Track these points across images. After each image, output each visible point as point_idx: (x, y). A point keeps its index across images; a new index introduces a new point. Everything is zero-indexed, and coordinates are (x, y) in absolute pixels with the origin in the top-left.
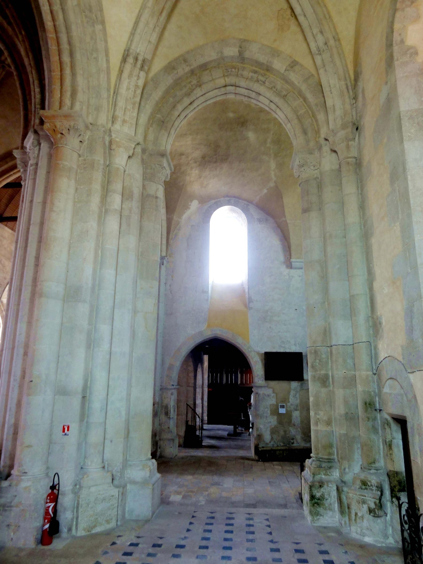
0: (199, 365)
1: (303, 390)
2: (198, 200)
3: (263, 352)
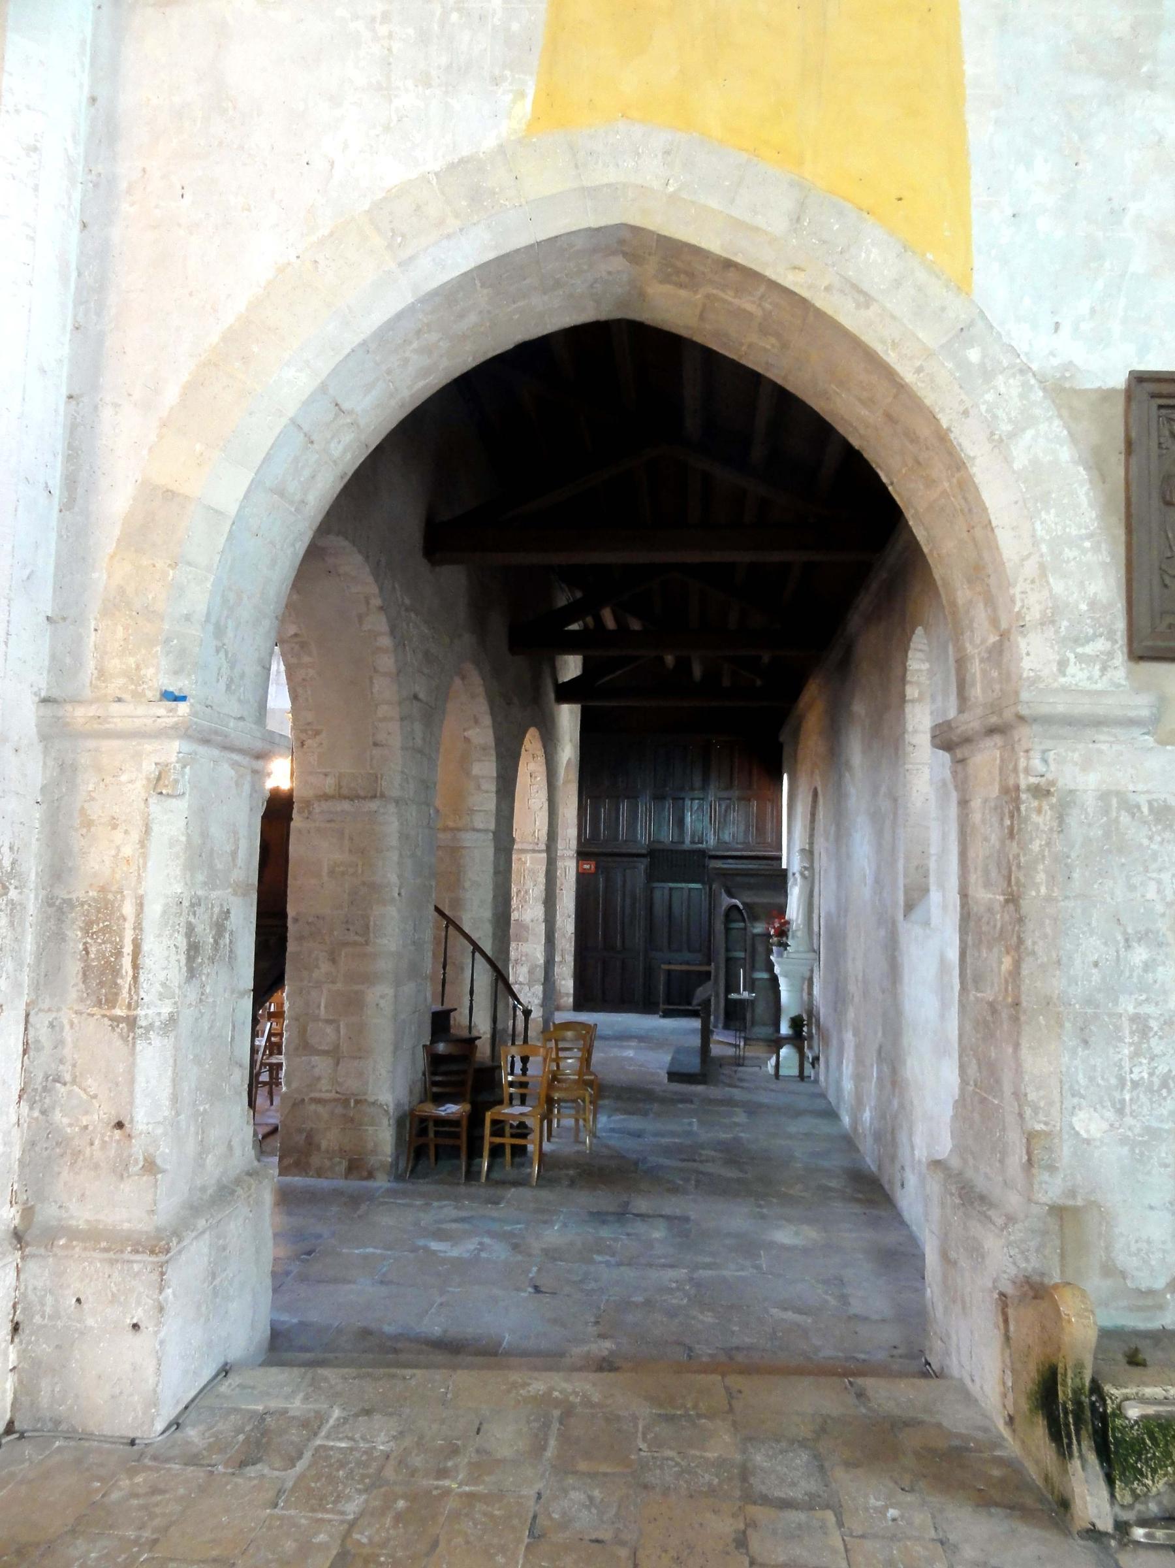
0: (532, 742)
3: (1118, 380)
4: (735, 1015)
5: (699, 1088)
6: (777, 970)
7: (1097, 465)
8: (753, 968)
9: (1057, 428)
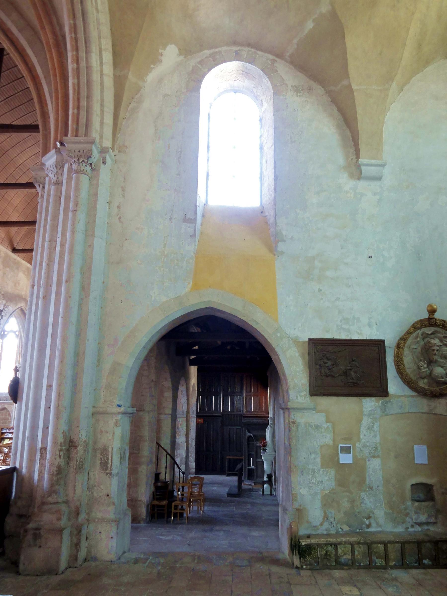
0: (182, 382)
1: (387, 415)
2: (176, 45)
3: (307, 340)
4: (251, 475)
5: (237, 499)
6: (263, 458)
7: (303, 356)
8: (257, 458)
9: (295, 349)
